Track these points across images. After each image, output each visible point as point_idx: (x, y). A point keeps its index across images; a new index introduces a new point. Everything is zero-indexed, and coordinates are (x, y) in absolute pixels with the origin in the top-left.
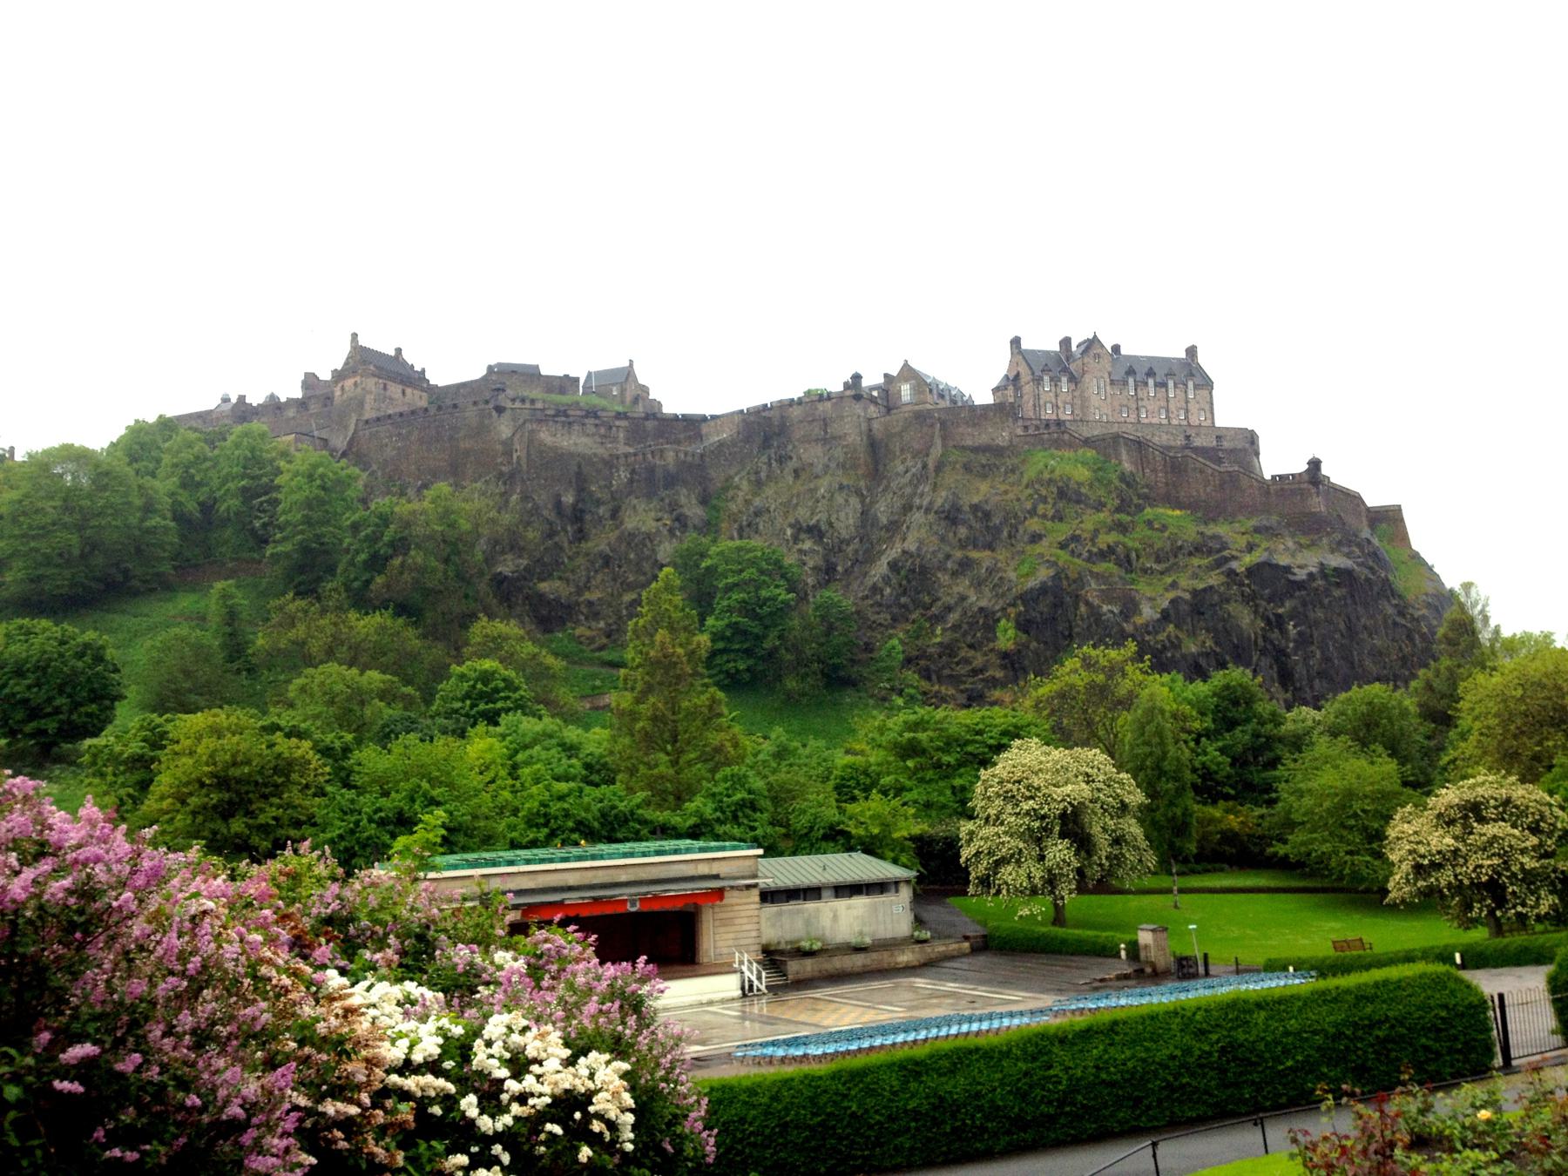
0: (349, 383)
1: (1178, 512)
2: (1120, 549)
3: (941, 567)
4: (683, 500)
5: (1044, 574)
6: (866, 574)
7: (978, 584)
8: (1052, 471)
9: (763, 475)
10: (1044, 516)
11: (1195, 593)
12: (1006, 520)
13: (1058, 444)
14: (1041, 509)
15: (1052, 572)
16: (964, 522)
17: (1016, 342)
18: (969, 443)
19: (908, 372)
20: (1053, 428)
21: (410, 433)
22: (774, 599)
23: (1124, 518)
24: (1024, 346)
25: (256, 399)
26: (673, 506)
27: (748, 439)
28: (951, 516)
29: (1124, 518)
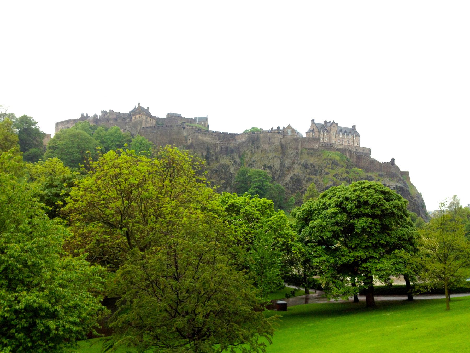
0: (137, 116)
1: (360, 170)
2: (347, 178)
3: (304, 179)
4: (235, 157)
6: (283, 180)
8: (330, 157)
9: (253, 151)
10: (329, 168)
12: (318, 168)
13: (330, 149)
14: (328, 166)
16: (309, 168)
17: (313, 121)
18: (308, 147)
19: (289, 127)
20: (329, 145)
21: (158, 132)
22: (267, 185)
23: (348, 170)
24: (315, 122)
25: (91, 115)
26: (233, 158)
27: (249, 141)
28: (306, 166)
29: (348, 170)
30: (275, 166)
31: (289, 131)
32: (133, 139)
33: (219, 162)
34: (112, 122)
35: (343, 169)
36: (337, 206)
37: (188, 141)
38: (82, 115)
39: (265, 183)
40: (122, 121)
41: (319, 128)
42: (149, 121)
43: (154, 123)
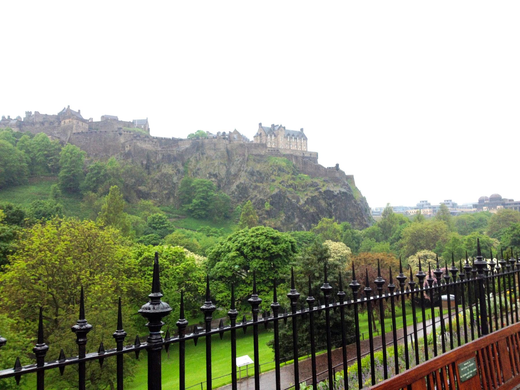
0: (67, 121)
1: (306, 176)
3: (250, 187)
4: (178, 165)
5: (276, 191)
7: (260, 192)
8: (277, 163)
11: (312, 197)
12: (265, 175)
13: (277, 155)
14: (274, 173)
15: (278, 190)
17: (260, 124)
19: (236, 132)
22: (212, 195)
25: (13, 117)
26: (176, 167)
27: (193, 148)
28: (252, 174)
30: (221, 174)
31: (235, 136)
32: (62, 148)
33: (161, 171)
34: (38, 126)
35: (289, 176)
36: (237, 250)
37: (126, 149)
38: (3, 117)
39: (209, 194)
40: (50, 125)
41: (267, 132)
42: (81, 125)
43: (87, 127)
